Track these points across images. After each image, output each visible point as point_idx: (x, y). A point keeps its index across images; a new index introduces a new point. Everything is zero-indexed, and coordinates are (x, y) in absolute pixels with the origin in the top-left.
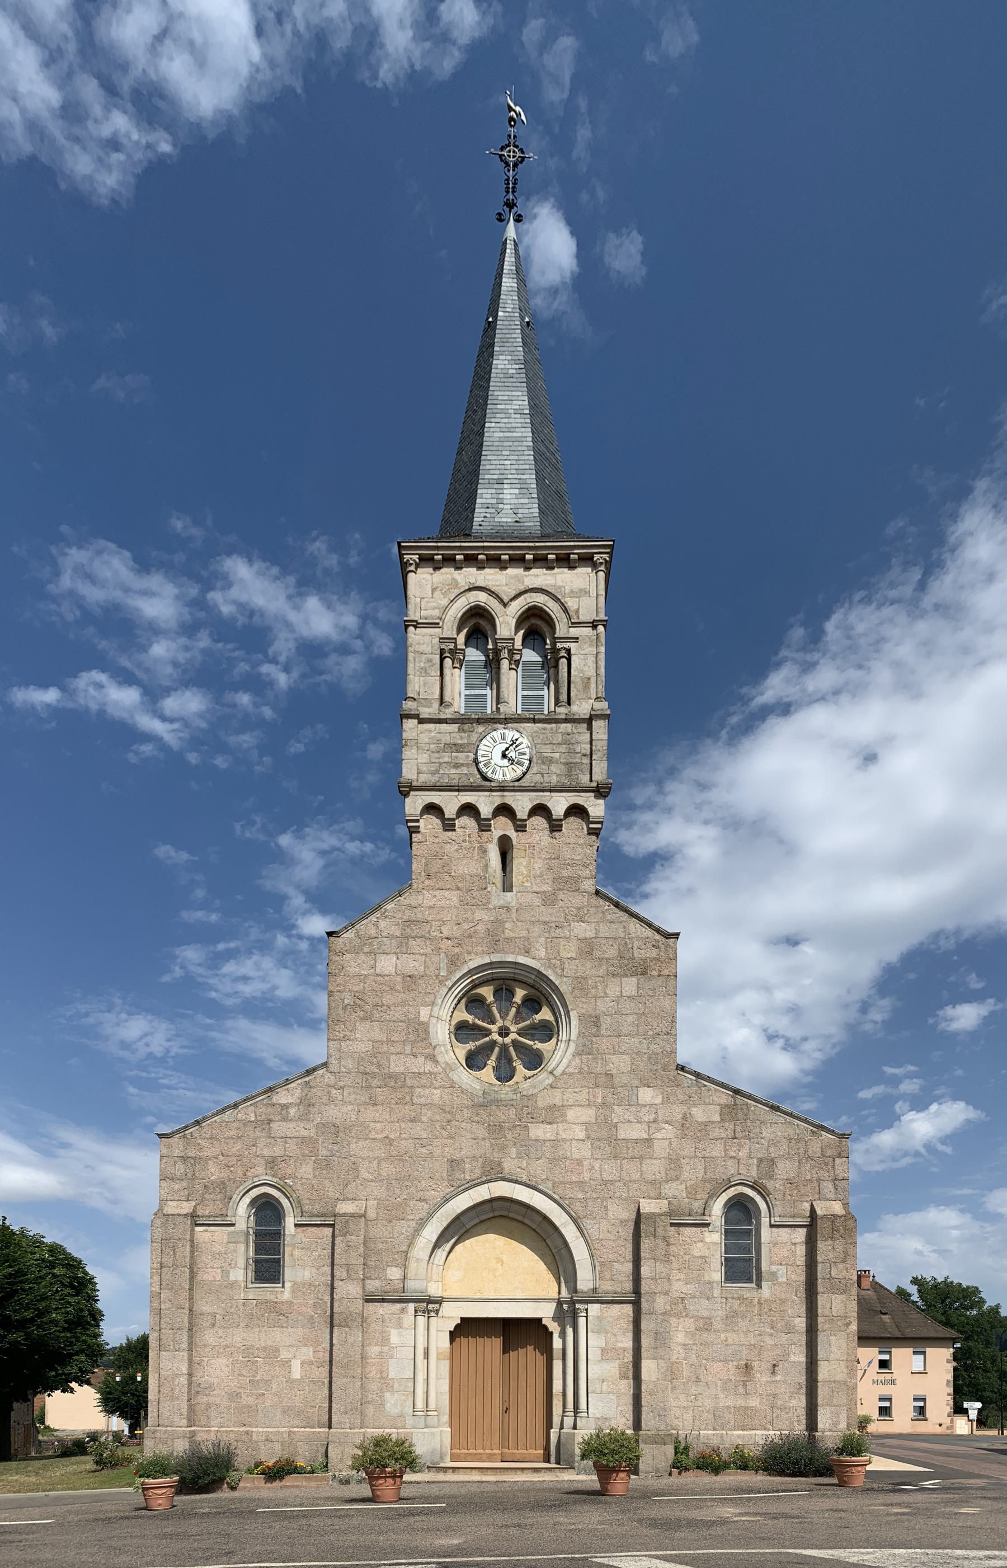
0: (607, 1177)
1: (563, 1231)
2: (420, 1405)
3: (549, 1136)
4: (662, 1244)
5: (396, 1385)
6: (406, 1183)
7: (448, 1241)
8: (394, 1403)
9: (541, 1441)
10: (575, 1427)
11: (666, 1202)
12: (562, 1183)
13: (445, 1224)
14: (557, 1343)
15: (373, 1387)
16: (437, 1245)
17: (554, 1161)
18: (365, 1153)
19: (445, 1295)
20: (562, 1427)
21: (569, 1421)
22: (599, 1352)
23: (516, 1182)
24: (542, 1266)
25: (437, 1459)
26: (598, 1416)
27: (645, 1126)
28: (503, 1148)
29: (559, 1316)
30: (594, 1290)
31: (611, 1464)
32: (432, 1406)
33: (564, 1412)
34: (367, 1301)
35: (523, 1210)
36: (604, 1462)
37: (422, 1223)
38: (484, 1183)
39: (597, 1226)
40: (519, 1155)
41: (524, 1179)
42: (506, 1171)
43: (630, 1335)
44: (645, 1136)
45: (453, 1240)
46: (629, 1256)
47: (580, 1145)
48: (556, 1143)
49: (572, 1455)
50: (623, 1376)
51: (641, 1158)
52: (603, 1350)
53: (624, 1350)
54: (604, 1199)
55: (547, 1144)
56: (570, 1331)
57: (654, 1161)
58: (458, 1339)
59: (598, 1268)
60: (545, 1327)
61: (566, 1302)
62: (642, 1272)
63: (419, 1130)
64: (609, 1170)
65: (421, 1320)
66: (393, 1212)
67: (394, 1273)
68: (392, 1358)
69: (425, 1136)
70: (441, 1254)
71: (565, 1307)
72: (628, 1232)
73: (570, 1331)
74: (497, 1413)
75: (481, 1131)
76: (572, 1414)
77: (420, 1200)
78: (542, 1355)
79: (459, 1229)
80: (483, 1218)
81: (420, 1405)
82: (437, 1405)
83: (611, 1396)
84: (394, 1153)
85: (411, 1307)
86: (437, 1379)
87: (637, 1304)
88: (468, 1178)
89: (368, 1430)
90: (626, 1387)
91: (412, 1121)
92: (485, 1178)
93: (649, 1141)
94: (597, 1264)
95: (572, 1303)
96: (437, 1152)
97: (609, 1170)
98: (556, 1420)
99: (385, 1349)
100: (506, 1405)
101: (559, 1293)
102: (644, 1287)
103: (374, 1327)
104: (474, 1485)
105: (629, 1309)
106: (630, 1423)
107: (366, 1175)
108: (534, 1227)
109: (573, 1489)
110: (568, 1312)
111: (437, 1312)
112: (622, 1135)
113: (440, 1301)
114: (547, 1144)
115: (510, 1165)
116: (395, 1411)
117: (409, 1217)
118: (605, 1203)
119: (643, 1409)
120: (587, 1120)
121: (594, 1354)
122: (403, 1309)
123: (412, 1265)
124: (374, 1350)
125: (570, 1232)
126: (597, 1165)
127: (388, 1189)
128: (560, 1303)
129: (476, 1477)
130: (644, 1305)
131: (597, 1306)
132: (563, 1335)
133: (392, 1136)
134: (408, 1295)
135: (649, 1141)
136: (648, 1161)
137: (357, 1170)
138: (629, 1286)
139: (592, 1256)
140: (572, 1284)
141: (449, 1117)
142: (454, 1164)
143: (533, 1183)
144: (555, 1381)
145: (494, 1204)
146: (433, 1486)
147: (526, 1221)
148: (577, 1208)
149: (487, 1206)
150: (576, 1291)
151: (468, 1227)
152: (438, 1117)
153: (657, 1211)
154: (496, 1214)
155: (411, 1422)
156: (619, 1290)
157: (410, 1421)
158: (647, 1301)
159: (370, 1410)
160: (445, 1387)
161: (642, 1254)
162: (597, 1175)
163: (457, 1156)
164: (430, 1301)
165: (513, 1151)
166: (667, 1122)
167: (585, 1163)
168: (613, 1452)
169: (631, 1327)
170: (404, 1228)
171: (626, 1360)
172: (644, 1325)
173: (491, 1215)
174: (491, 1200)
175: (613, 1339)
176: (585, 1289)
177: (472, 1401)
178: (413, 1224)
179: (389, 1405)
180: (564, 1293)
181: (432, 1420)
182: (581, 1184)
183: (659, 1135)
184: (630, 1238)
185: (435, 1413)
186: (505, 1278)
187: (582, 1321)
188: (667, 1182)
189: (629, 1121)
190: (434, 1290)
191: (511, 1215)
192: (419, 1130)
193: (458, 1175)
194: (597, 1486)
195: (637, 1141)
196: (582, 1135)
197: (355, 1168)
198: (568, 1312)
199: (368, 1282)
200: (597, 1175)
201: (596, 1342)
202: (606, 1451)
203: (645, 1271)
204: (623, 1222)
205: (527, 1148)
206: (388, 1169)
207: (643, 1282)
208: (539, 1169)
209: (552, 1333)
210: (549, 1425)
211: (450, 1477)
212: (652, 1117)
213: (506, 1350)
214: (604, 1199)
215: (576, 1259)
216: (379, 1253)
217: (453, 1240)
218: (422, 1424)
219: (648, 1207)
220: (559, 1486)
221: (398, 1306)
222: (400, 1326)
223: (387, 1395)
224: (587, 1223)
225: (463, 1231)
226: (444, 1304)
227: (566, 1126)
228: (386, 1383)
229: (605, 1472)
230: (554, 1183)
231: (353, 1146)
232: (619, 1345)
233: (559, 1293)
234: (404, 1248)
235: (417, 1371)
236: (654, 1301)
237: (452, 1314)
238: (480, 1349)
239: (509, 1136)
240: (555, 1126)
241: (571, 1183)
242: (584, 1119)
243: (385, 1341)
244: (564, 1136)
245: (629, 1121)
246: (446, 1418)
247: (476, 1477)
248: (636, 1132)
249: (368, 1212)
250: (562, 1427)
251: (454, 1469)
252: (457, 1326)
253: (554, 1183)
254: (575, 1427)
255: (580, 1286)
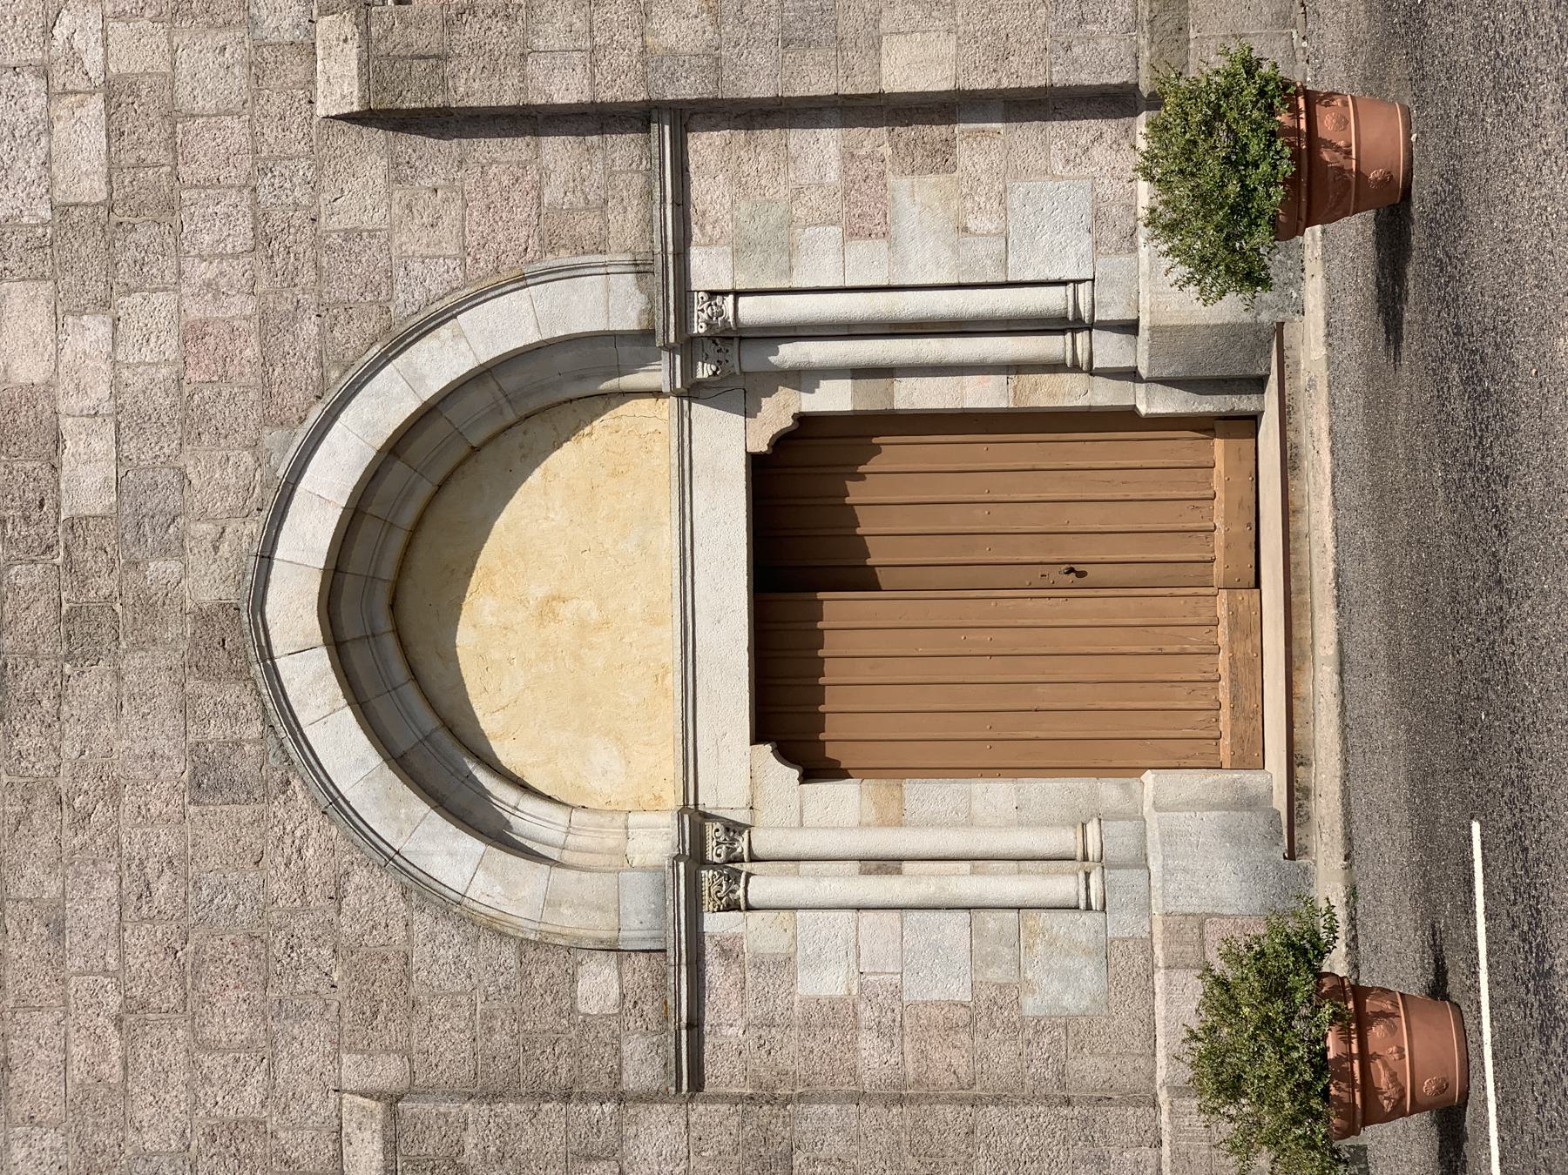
0: (241, 234)
1: (435, 384)
2: (1064, 886)
3: (103, 445)
4: (470, 31)
5: (995, 974)
6: (278, 949)
7: (484, 794)
8: (1061, 982)
9: (1184, 447)
10: (1129, 328)
11: (323, 23)
12: (267, 393)
13: (421, 808)
14: (834, 398)
15: (1002, 1058)
16: (498, 835)
17: (191, 422)
18: (177, 1098)
19: (673, 800)
20: (1132, 375)
21: (1109, 350)
22: (860, 248)
23: (266, 558)
24: (566, 461)
25: (1259, 821)
26: (1087, 240)
27: (61, 109)
28: (148, 607)
29: (739, 391)
30: (641, 269)
31: (1286, 167)
32: (1066, 840)
33: (1076, 368)
34: (697, 1082)
35: (368, 529)
36: (1278, 194)
37: (420, 888)
38: (272, 673)
39: (416, 268)
40: (176, 549)
41: (255, 527)
42: (228, 593)
43: (798, 137)
44: (96, 104)
45: (482, 776)
46: (516, 148)
47: (131, 333)
48: (125, 419)
49: (1231, 332)
50: (943, 160)
51: (172, 115)
52: (852, 234)
53: (849, 156)
54: (318, 242)
55: (129, 448)
56: (790, 354)
57: (184, 69)
58: (831, 752)
59: (565, 258)
60: (782, 441)
61: (688, 369)
62: (571, 98)
63: (93, 905)
64: (218, 226)
65: (763, 886)
66: (381, 995)
67: (598, 987)
68: (898, 991)
69: (110, 886)
70: (528, 818)
71: (704, 371)
72: (433, 155)
73: (790, 354)
74: (1086, 607)
75: (92, 684)
76: (1082, 338)
77: (337, 898)
78: (877, 450)
79: (441, 755)
80: (399, 671)
81: (1064, 886)
82: (1063, 823)
83: (1014, 201)
84: (173, 997)
85: (715, 923)
86: (970, 823)
87: (686, 117)
88: (256, 729)
89: (1161, 1075)
90: (980, 147)
91: (58, 930)
92: (257, 669)
93: (114, 92)
94: (551, 261)
95: (689, 347)
96: (167, 840)
97: (218, 226)
98: (1105, 395)
99: (867, 1014)
100: (1056, 575)
101: (657, 394)
102: (624, 90)
103: (790, 1054)
104: (1356, 685)
105: (705, 146)
106: (1109, 128)
107: (252, 1093)
108: (425, 489)
109: (1372, 322)
110: (725, 360)
111: (733, 829)
112: (92, 188)
113: (695, 819)
114: (129, 448)
115: (208, 582)
116: (1090, 976)
117: (399, 934)
118: (336, 240)
119: (1059, 79)
120: (42, 311)
121: (868, 264)
122: (725, 953)
123: (570, 922)
124: (873, 1058)
125: (439, 363)
126: (201, 271)
127: (301, 1014)
128: (693, 391)
129: (1322, 680)
130: (688, 88)
131: (696, 257)
132: (803, 378)
133: (114, 1001)
134: (675, 939)
135: (114, 92)
136: (183, 93)
137: (234, 1128)
138: (623, 148)
139: (522, 281)
140: (625, 350)
141: (41, 801)
142: (208, 779)
143: (271, 497)
144: (970, 404)
145: (350, 630)
146: (1365, 841)
147: (408, 517)
148: (354, 337)
149: (360, 658)
150: (646, 335)
151: (429, 722)
152: (45, 841)
153: (352, 50)
154: (384, 623)
155: (1127, 917)
156: (639, 181)
157: (1123, 923)
158: (672, 79)
159: (1090, 1069)
160: (995, 794)
161: (509, 100)
162: (236, 271)
163: (180, 769)
164: (694, 856)
165: (161, 569)
166: (48, 31)
167: (194, 312)
168: (1237, 161)
169: (768, 136)
170: (437, 953)
171: (887, 150)
172: (760, 88)
173: (390, 642)
174: (336, 643)
175: (813, 198)
176: (638, 301)
177: (1045, 696)
178: (423, 922)
179: (1068, 1000)
180: (656, 375)
181: (1120, 839)
182: (270, 325)
183: (93, 58)
184: (452, 147)
185: (1092, 829)
186: (609, 590)
187: (753, 311)
188: (253, 23)
189: (47, 163)
190: (656, 840)
191: (388, 570)
192: (93, 905)
193: (246, 765)
194: (1356, 229)
195: (113, 134)
196: (96, 328)
197: (225, 1133)
198: (725, 360)
199: (630, 1082)
200: (236, 271)
201: (824, 258)
202: (1233, 188)
203: (566, 89)
204: (398, 174)
205: (144, 518)
206: (230, 1020)
207: (607, 96)
208: (220, 477)
209: (802, 419)
210: (1125, 419)
211: (1325, 774)
212: (33, 84)
213: (863, 579)
214: (318, 242)
215: (531, 337)
216: (526, 1043)
217: (482, 776)
218: (1137, 876)
219: (340, 87)
220: (1355, 376)
221: (714, 969)
222: (785, 964)
223: (1031, 1005)
224: (407, 302)
225: (446, 741)
226: (707, 802)
227: (66, 384)
228: (990, 1011)
229: (1316, 190)
230: (266, 421)
231: (151, 1140)
232: (832, 176)
233: (657, 394)
234: (509, 953)
235: (944, 898)
236: (673, 53)
237: (741, 773)
238: (863, 671)
239: (106, 584)
240: (67, 424)
241: (266, 362)
242: (40, 320)
243: (836, 1017)
244: (103, 390)
245: (47, 163)
246: (1109, 790)
247: (1322, 680)
248: (83, 137)
249: (368, 1083)
250: (1132, 375)
251: (1294, 759)
252: (786, 755)
253: (266, 421)
254: (1129, 328)
255: (627, 319)
